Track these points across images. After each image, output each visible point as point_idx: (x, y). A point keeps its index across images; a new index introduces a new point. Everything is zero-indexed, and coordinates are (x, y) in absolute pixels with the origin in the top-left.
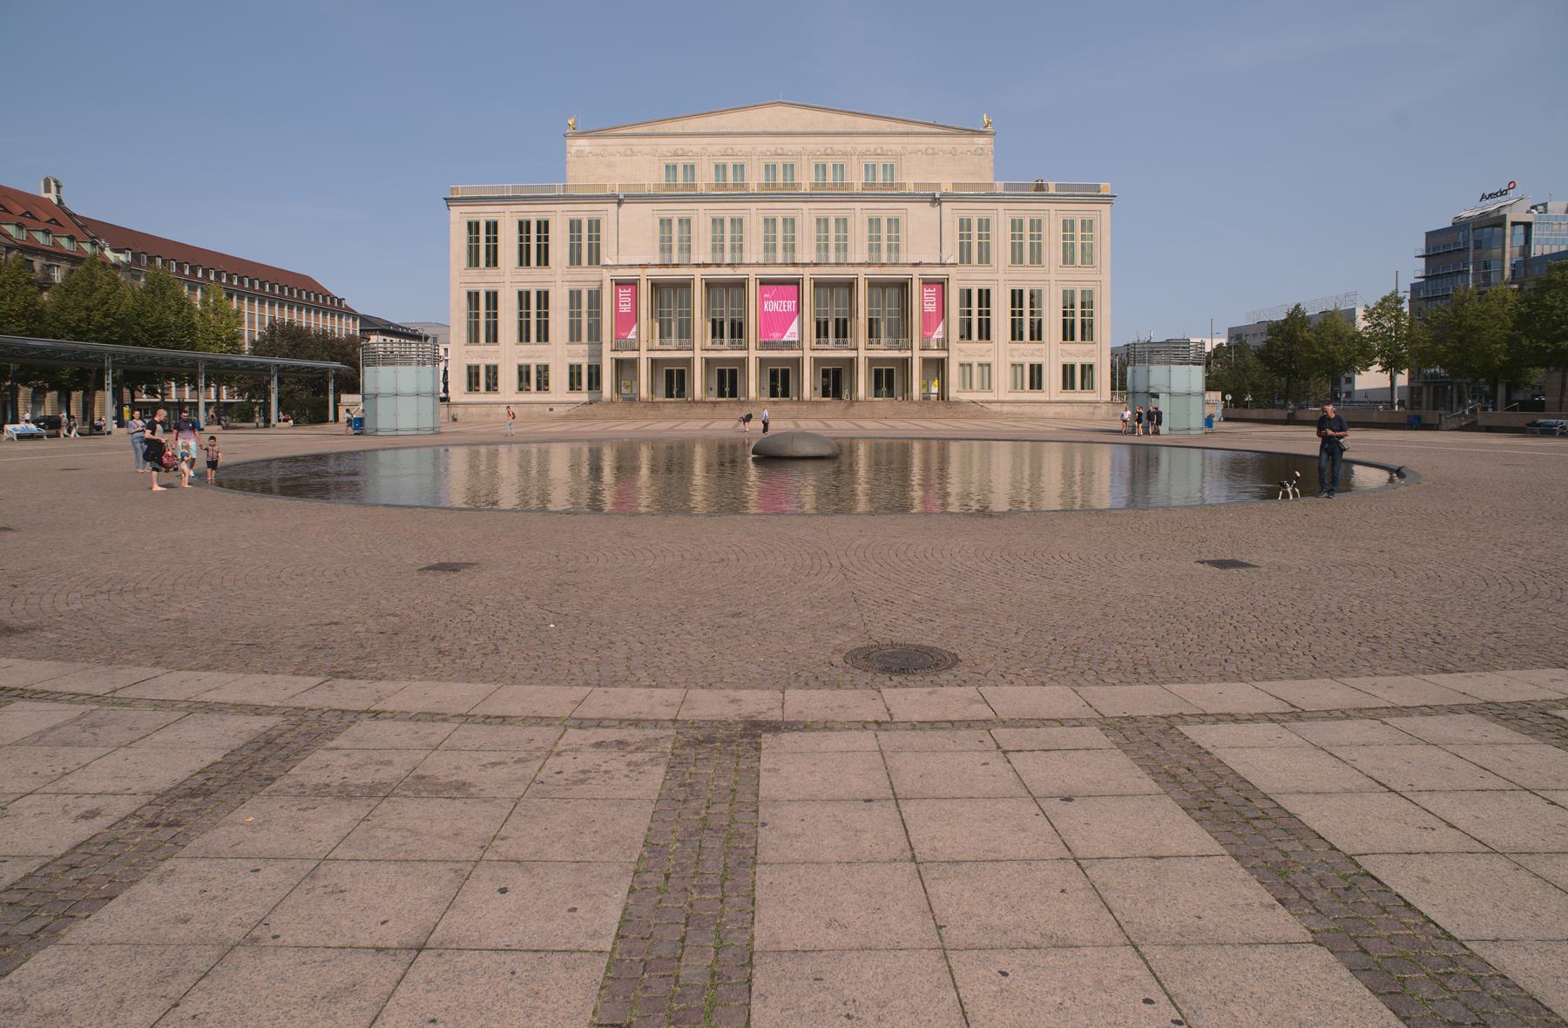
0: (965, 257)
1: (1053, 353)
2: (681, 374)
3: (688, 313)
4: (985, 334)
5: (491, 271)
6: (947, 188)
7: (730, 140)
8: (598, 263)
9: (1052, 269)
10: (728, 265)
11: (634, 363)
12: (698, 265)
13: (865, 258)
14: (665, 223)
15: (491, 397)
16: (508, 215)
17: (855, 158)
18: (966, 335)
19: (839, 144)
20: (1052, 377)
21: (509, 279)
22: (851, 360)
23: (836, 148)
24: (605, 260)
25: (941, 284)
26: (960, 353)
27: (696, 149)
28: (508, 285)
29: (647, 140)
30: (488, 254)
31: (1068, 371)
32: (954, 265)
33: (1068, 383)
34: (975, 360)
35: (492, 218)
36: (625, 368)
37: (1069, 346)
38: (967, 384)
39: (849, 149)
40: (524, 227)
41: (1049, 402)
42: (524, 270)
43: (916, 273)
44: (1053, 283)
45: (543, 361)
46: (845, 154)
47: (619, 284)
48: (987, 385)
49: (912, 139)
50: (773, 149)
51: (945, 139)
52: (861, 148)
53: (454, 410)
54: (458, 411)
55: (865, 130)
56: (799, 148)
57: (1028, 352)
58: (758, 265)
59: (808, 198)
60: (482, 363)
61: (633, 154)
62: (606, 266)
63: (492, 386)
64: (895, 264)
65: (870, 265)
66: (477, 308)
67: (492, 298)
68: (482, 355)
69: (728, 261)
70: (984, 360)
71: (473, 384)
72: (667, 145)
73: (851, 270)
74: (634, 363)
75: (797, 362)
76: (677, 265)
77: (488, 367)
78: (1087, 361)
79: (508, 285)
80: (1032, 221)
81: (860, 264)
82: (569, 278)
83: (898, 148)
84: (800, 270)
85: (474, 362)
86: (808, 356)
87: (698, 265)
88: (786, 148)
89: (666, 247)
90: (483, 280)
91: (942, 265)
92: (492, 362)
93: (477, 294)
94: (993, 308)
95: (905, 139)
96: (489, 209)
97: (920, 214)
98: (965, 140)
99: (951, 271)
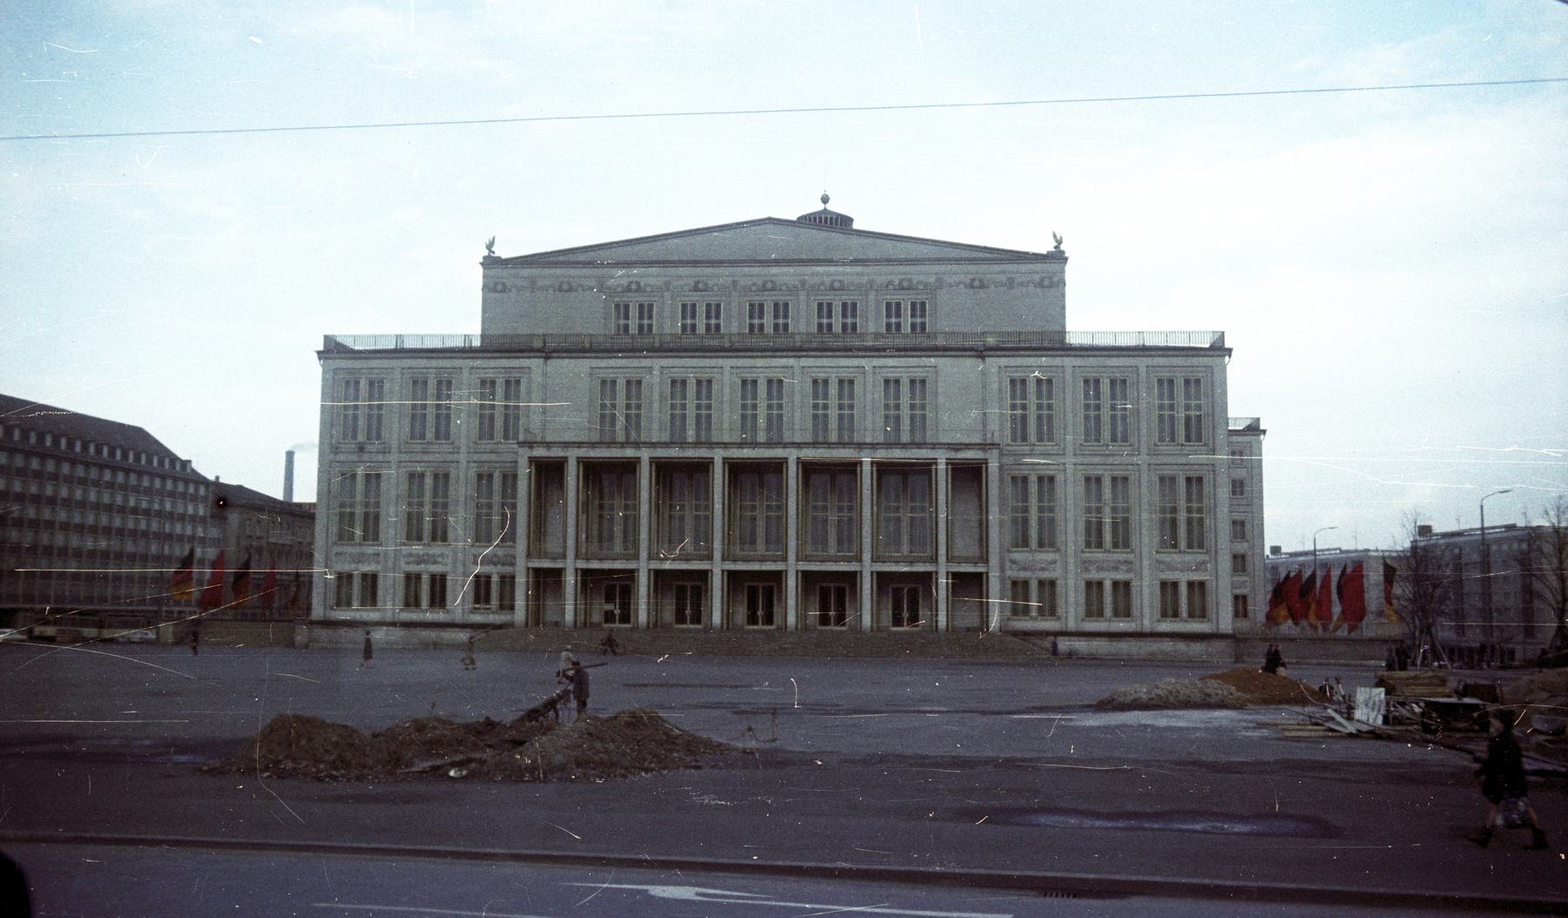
3: (707, 508)
11: (558, 573)
14: (608, 385)
34: (1033, 577)
48: (1050, 610)
52: (880, 280)
59: (798, 350)
64: (919, 446)
70: (1046, 575)
74: (558, 573)
97: (952, 373)
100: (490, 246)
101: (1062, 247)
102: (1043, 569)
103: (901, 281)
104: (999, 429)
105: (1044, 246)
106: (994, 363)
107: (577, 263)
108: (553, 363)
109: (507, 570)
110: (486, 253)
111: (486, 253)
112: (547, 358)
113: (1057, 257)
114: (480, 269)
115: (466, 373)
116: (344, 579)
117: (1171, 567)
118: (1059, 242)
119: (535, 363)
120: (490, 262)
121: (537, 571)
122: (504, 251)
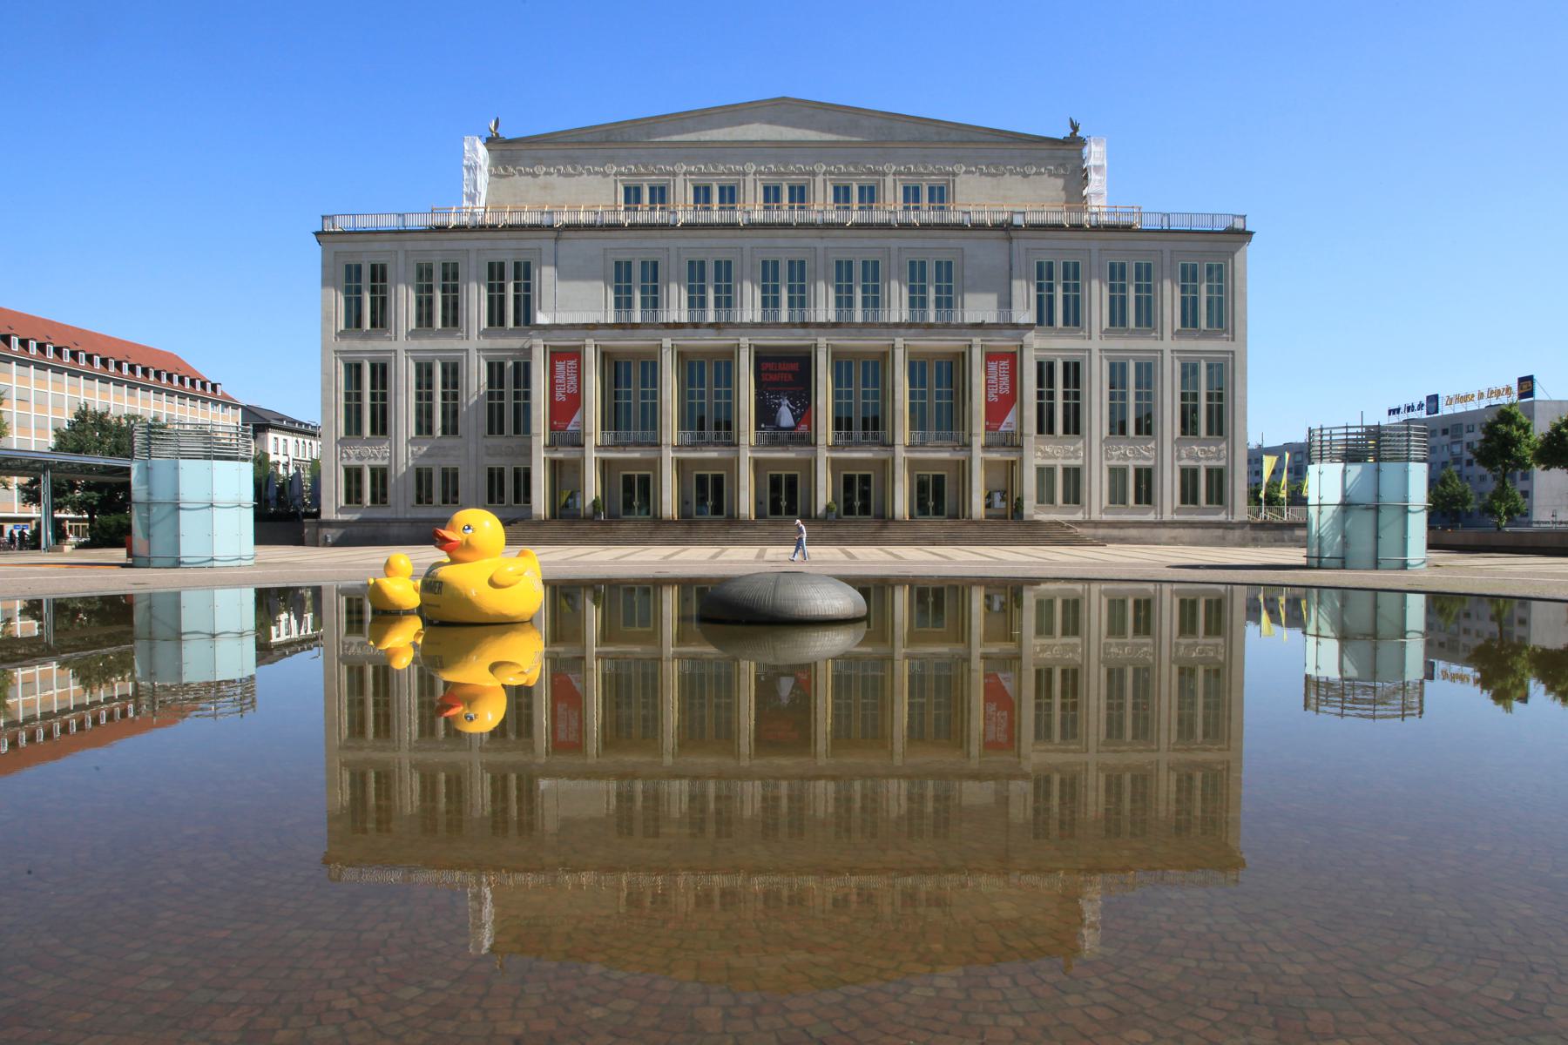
0: (1045, 316)
1: (1169, 456)
2: (645, 480)
4: (1074, 425)
6: (1018, 220)
8: (527, 322)
10: (710, 325)
12: (667, 326)
13: (905, 317)
16: (401, 257)
18: (1045, 425)
20: (1169, 486)
22: (884, 462)
24: (541, 318)
25: (1013, 359)
26: (1038, 454)
30: (373, 312)
31: (1189, 478)
32: (1029, 327)
33: (1188, 495)
36: (564, 475)
38: (1046, 497)
45: (450, 463)
57: (1132, 454)
58: (753, 325)
66: (359, 385)
67: (381, 372)
69: (711, 318)
80: (1138, 266)
89: (624, 303)
90: (367, 347)
94: (1084, 388)
96: (376, 246)
104: (1024, 313)
105: (1063, 132)
106: (1021, 244)
118: (1075, 128)
122: (507, 133)
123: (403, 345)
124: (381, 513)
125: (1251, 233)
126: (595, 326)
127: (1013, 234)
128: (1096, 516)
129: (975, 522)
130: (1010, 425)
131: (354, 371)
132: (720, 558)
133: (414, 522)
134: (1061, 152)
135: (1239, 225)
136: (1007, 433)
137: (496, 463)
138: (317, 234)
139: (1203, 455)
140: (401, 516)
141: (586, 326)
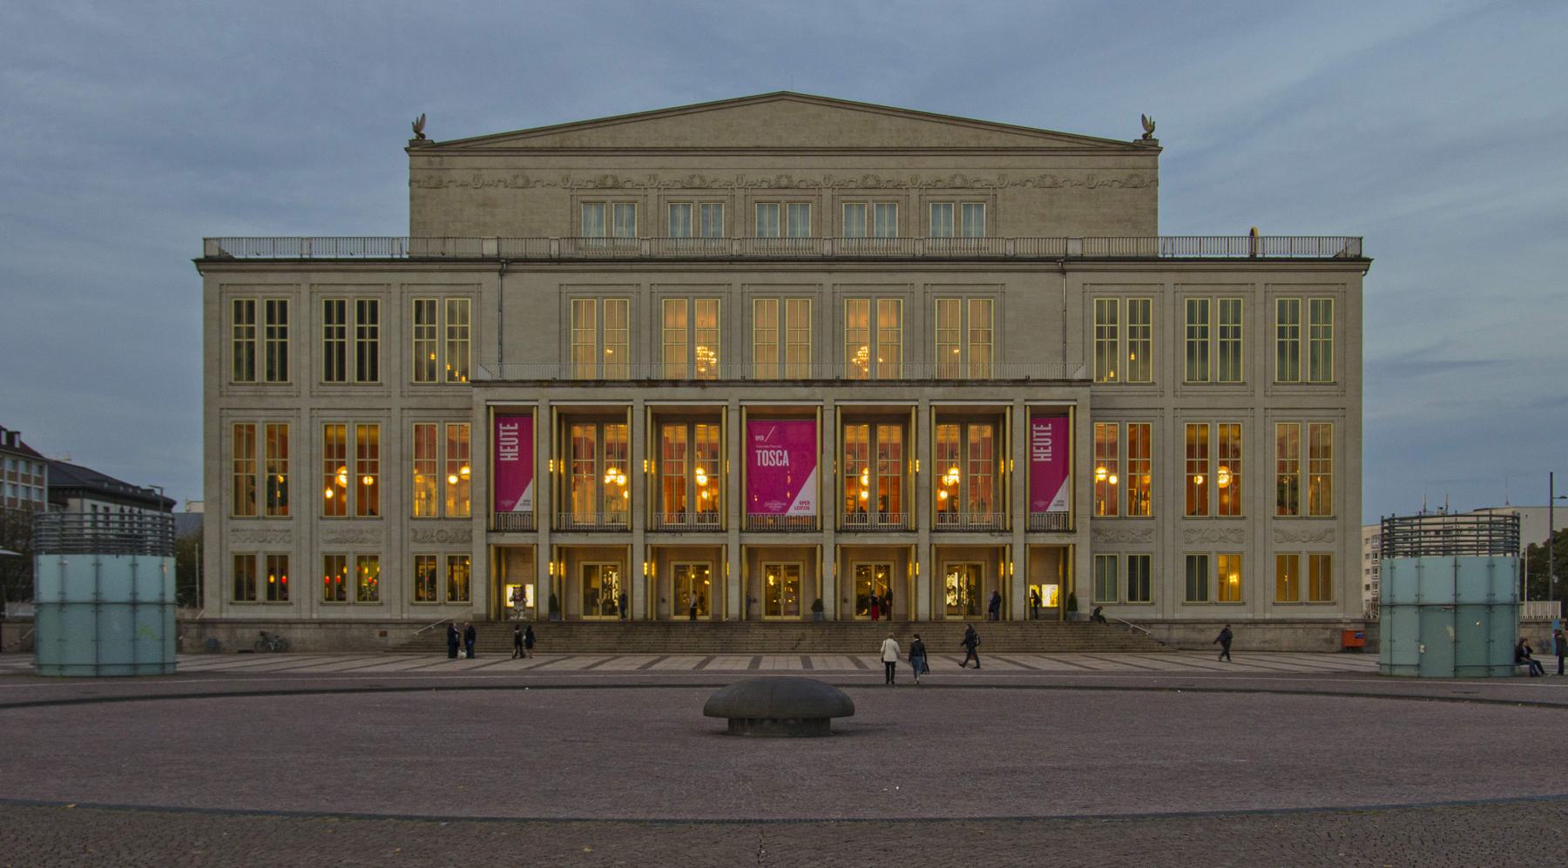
5: (276, 389)
6: (1075, 249)
7: (696, 161)
9: (1259, 390)
12: (639, 383)
15: (276, 612)
17: (914, 194)
19: (888, 169)
21: (306, 403)
23: (884, 176)
27: (637, 177)
28: (305, 415)
29: (553, 161)
30: (270, 361)
32: (1086, 382)
35: (277, 297)
37: (1289, 525)
39: (905, 177)
40: (334, 311)
41: (1254, 623)
42: (335, 388)
43: (1019, 395)
44: (1259, 412)
46: (897, 187)
47: (503, 416)
49: (1016, 161)
50: (772, 177)
51: (1074, 161)
52: (925, 177)
53: (210, 633)
54: (222, 635)
55: (934, 143)
56: (818, 177)
60: (261, 550)
61: (527, 184)
62: (476, 383)
63: (278, 593)
65: (938, 383)
68: (257, 536)
70: (1139, 550)
71: (243, 590)
72: (586, 169)
73: (907, 392)
75: (811, 553)
76: (600, 383)
77: (271, 559)
78: (1321, 548)
79: (305, 415)
81: (922, 383)
82: (414, 402)
83: (992, 177)
84: (818, 392)
85: (248, 548)
86: (828, 541)
87: (639, 383)
88: (797, 176)
91: (1068, 382)
92: (277, 548)
93: (251, 428)
95: (1004, 161)
98: (1108, 161)
99: (1083, 392)
100: (418, 128)
101: (1154, 135)
102: (1135, 541)
103: (954, 177)
105: (1134, 133)
106: (1075, 279)
107: (533, 150)
108: (511, 282)
109: (457, 549)
110: (414, 136)
111: (414, 136)
112: (502, 273)
113: (1147, 146)
114: (406, 157)
115: (395, 291)
116: (244, 563)
117: (1291, 539)
118: (1149, 127)
119: (490, 279)
120: (420, 145)
121: (499, 549)
122: (434, 134)
123: (306, 403)
124: (276, 612)
125: (1369, 260)
126: (551, 383)
127: (1066, 267)
128: (1168, 616)
129: (1017, 623)
130: (1061, 503)
131: (245, 435)
132: (708, 667)
133: (322, 623)
134: (1129, 160)
135: (1352, 252)
136: (1058, 515)
137: (426, 549)
138: (197, 261)
139: (1302, 537)
140: (305, 616)
141: (540, 383)
